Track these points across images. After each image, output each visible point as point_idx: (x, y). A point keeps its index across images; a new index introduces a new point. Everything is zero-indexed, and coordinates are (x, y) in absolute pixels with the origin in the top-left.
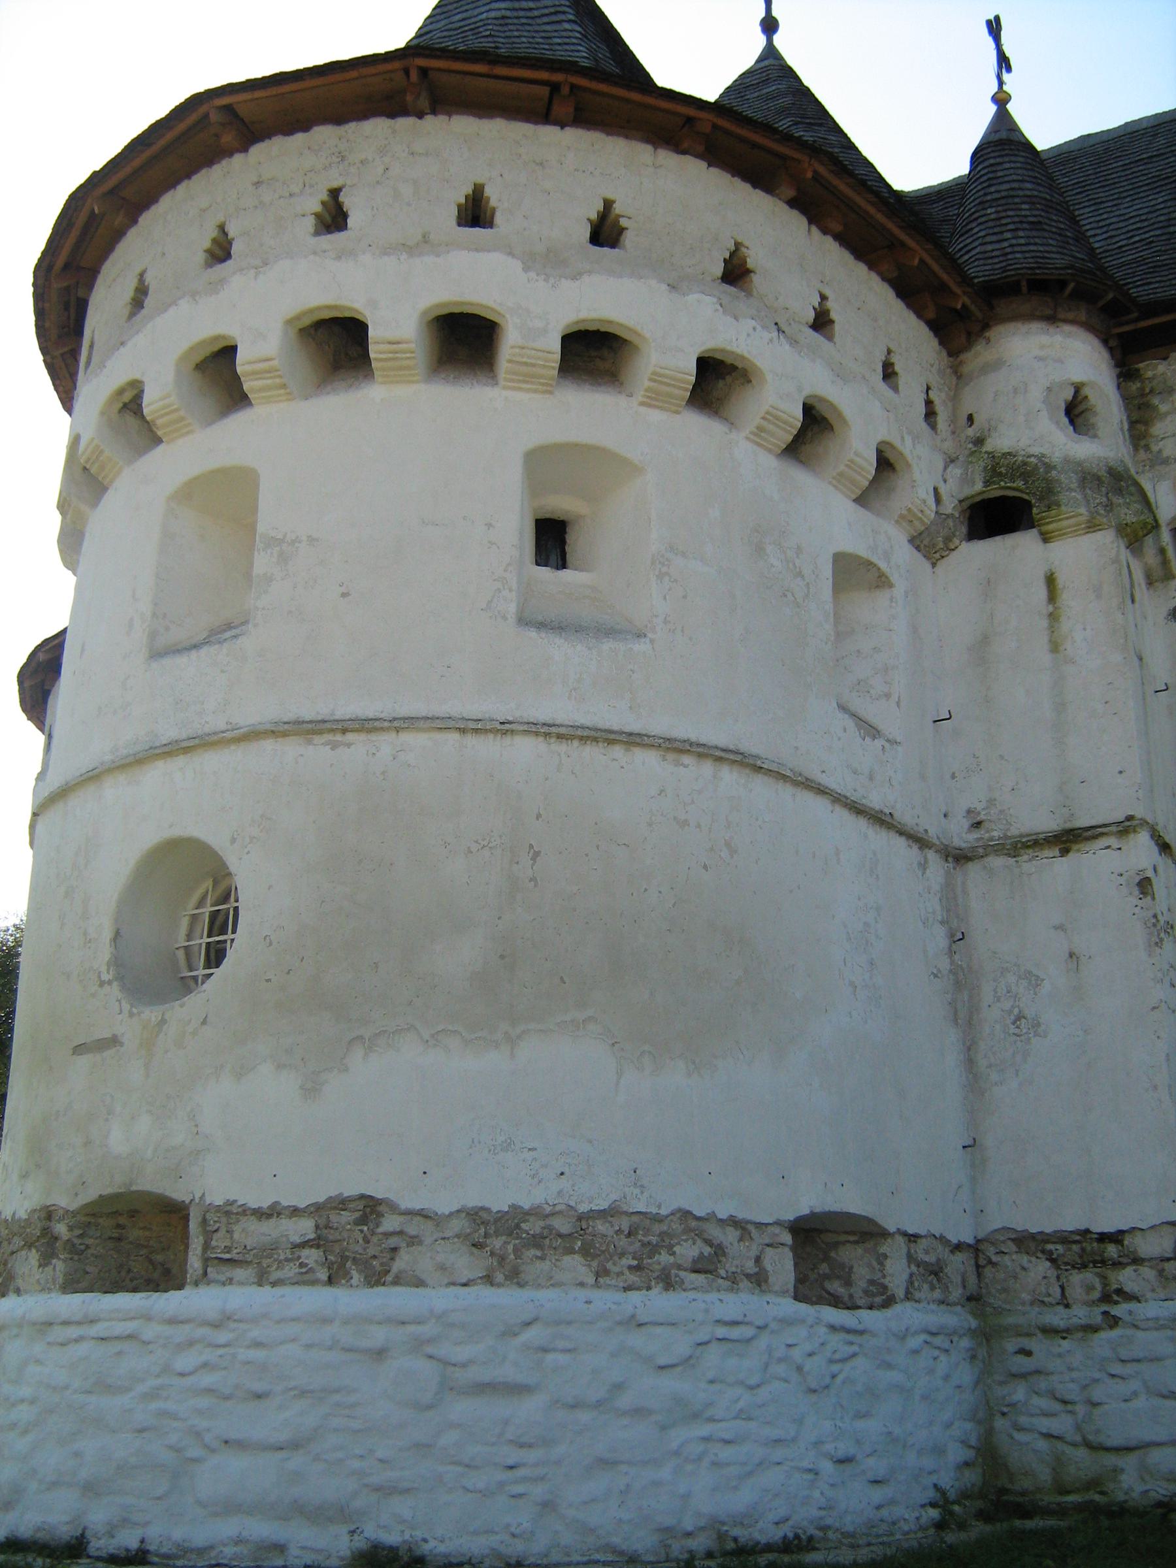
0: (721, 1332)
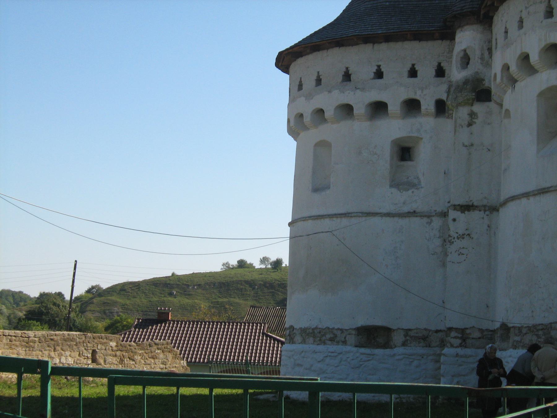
0: (330, 354)
